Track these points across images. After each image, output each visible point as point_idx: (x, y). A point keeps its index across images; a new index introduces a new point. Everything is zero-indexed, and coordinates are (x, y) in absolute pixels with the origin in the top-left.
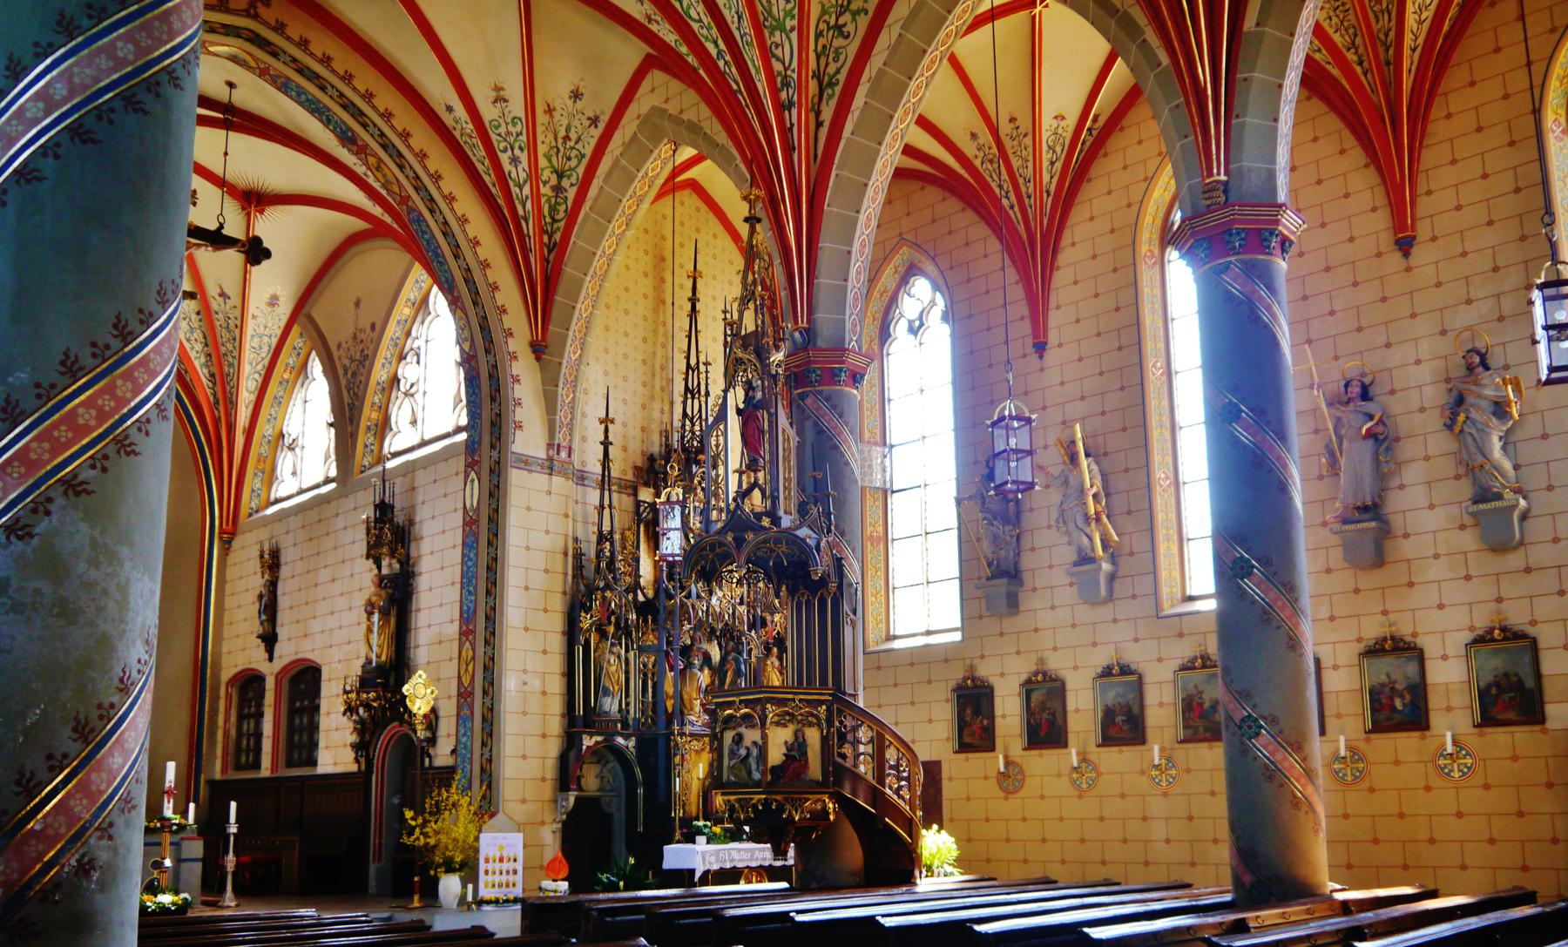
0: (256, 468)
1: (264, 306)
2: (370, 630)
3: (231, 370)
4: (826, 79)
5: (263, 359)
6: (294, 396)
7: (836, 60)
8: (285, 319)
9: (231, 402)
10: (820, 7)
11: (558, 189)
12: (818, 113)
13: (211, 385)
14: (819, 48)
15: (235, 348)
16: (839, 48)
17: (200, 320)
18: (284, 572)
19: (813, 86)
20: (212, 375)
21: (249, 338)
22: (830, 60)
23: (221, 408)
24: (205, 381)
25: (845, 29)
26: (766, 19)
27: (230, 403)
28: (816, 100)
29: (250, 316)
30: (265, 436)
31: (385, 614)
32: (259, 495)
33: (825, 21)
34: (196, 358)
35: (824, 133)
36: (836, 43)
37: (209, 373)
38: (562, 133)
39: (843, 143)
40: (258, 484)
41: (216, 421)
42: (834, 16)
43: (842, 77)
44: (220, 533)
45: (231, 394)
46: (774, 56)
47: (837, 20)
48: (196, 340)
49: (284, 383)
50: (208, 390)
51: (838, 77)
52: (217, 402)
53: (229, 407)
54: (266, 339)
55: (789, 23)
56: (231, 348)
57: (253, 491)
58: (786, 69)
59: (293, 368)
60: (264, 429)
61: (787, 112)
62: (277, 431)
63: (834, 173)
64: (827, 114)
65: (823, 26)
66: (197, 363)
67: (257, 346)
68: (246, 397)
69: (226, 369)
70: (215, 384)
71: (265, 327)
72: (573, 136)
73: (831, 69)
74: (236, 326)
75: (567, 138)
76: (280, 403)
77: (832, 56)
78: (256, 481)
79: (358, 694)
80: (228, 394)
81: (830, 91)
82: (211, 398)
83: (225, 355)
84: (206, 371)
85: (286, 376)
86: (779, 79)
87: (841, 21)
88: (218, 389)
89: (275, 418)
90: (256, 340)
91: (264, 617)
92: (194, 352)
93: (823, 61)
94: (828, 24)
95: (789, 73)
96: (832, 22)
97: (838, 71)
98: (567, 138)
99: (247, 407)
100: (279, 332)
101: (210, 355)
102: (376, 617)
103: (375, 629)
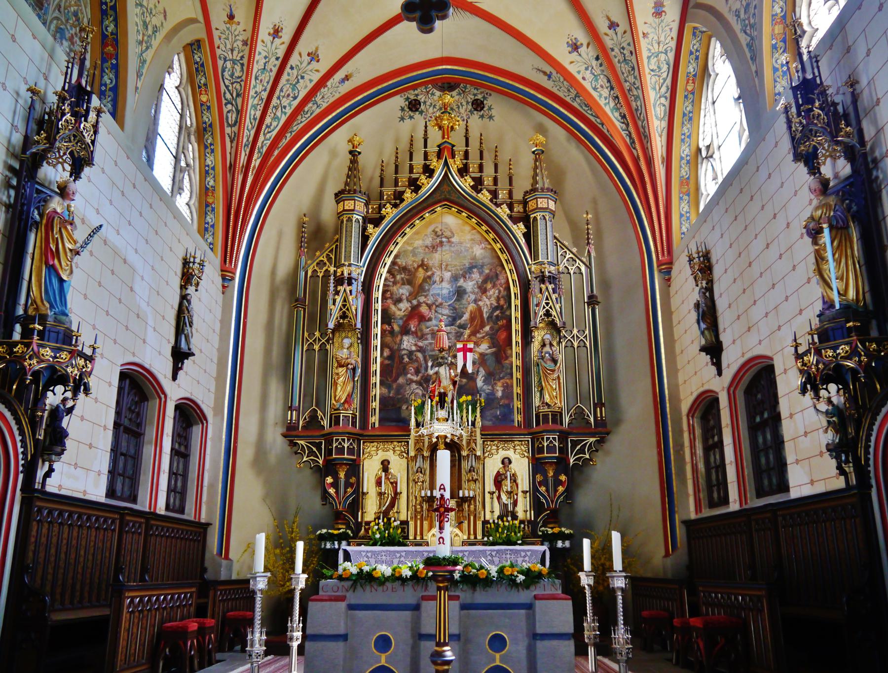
0: (680, 192)
1: (651, 19)
2: (820, 258)
3: (639, 104)
5: (665, 80)
6: (703, 107)
8: (675, 26)
9: (646, 137)
13: (624, 126)
15: (635, 78)
17: (601, 65)
18: (717, 271)
20: (624, 117)
21: (645, 61)
23: (638, 146)
24: (618, 124)
27: (644, 137)
29: (641, 35)
30: (682, 158)
31: (839, 230)
32: (688, 218)
34: (605, 105)
37: (620, 116)
40: (685, 207)
41: (636, 160)
44: (658, 266)
45: (643, 128)
48: (602, 87)
49: (691, 96)
50: (623, 133)
52: (634, 142)
53: (645, 142)
54: (663, 57)
56: (633, 80)
57: (681, 215)
59: (695, 75)
60: (681, 150)
62: (694, 148)
66: (607, 109)
67: (655, 68)
68: (657, 126)
69: (634, 104)
70: (627, 125)
71: (659, 43)
74: (631, 53)
76: (690, 119)
78: (683, 205)
79: (818, 352)
80: (641, 130)
82: (628, 140)
83: (630, 90)
84: (617, 114)
85: (690, 88)
88: (632, 129)
89: (689, 137)
90: (653, 61)
91: (703, 326)
92: (603, 99)
99: (661, 136)
100: (673, 44)
101: (617, 97)
102: (826, 237)
103: (829, 254)
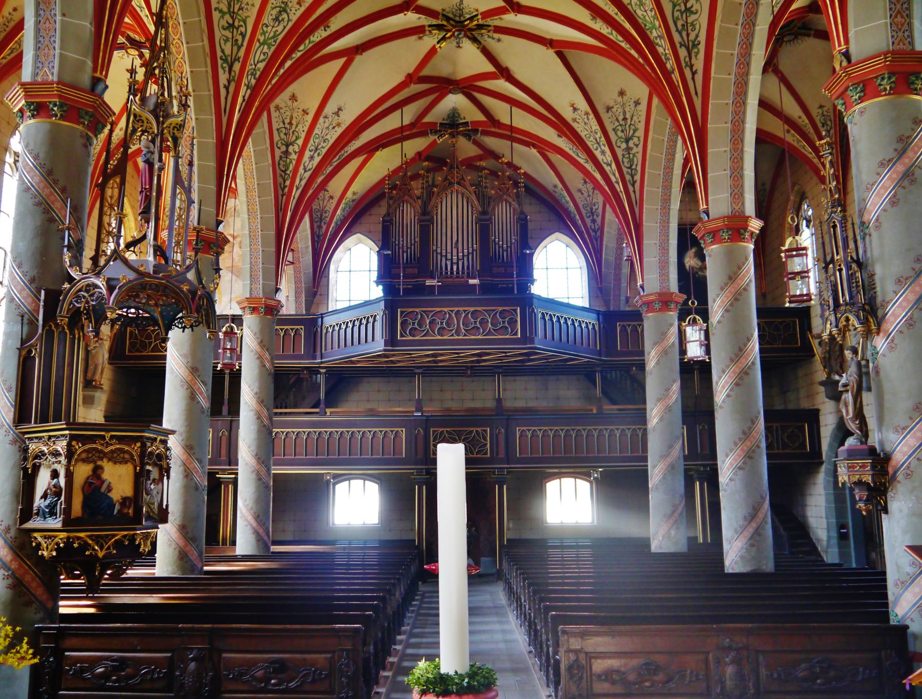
4: (691, 44)
7: (694, 29)
10: (671, 4)
11: (628, 149)
12: (691, 66)
14: (680, 27)
16: (693, 22)
19: (683, 52)
22: (690, 31)
25: (693, 9)
26: (645, 25)
28: (687, 59)
33: (677, 11)
35: (699, 77)
36: (690, 20)
38: (621, 118)
39: (712, 81)
42: (682, 5)
43: (702, 38)
46: (657, 44)
47: (685, 6)
51: (698, 39)
55: (657, 23)
58: (665, 50)
61: (673, 75)
63: (710, 102)
64: (699, 64)
65: (677, 14)
72: (628, 116)
73: (692, 37)
75: (625, 119)
77: (690, 28)
81: (696, 50)
86: (663, 57)
87: (689, 5)
93: (684, 34)
94: (680, 11)
95: (667, 51)
96: (683, 8)
97: (697, 36)
98: (625, 119)
